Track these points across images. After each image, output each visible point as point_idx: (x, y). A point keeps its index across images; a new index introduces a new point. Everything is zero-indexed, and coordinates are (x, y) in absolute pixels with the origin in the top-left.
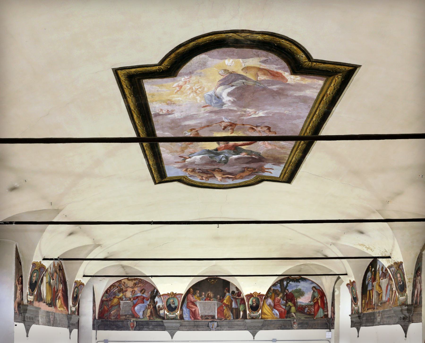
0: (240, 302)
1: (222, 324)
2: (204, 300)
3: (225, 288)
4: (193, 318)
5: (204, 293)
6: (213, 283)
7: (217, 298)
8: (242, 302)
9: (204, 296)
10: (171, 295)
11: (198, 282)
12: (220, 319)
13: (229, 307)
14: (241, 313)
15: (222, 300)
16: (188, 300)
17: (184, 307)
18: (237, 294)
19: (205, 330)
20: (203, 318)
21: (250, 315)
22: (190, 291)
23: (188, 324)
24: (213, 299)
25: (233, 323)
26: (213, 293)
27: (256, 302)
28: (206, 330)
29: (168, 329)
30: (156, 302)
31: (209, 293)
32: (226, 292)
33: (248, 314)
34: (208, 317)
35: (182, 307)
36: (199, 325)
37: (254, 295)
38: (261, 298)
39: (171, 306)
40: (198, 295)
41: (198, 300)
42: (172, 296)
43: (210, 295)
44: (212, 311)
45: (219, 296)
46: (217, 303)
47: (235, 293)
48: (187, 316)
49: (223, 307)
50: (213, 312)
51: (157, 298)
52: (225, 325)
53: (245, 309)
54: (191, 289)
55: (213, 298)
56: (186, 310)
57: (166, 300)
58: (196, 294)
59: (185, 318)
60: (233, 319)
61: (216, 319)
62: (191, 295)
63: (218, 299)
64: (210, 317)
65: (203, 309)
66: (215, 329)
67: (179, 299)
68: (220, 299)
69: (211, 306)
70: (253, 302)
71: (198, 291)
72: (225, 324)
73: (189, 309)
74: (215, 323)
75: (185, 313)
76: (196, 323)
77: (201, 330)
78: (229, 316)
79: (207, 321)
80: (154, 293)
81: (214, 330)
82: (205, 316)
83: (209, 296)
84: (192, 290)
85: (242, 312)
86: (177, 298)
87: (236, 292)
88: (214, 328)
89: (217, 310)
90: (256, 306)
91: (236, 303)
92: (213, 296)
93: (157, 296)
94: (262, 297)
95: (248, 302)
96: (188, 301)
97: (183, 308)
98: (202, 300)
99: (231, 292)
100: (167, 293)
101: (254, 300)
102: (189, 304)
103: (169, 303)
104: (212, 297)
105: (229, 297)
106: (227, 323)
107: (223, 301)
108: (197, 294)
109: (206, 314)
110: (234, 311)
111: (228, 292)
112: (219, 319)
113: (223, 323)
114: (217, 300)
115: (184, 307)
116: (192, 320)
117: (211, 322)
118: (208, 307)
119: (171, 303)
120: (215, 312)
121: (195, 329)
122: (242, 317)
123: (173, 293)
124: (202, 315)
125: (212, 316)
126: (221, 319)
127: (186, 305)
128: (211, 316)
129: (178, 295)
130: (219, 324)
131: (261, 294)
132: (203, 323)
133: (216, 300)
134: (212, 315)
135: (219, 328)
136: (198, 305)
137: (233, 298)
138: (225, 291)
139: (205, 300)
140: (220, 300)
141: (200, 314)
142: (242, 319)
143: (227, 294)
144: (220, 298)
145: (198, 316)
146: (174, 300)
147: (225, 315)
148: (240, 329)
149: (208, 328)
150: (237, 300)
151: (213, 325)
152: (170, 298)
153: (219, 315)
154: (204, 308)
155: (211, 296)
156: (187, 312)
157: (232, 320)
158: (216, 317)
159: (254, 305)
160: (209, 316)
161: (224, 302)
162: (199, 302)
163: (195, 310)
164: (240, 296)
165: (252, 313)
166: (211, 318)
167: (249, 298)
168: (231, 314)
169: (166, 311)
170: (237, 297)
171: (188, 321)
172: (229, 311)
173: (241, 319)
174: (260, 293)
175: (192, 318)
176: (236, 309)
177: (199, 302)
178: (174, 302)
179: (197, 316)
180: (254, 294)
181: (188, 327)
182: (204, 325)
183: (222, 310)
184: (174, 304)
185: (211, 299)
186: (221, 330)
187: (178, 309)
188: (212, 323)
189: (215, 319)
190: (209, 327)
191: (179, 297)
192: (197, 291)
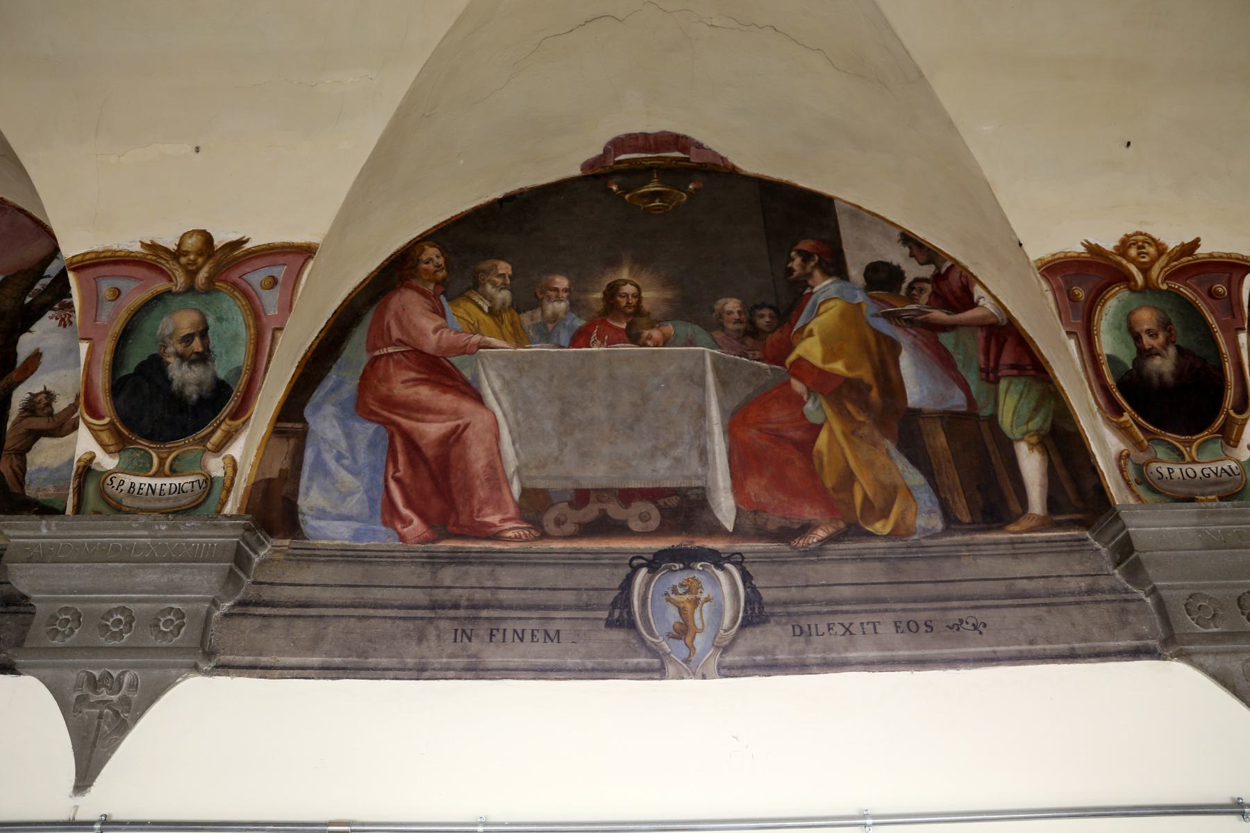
0: (987, 352)
1: (810, 593)
2: (565, 337)
3: (796, 244)
4: (416, 521)
5: (562, 282)
6: (657, 208)
7: (713, 324)
8: (998, 357)
9: (561, 306)
10: (184, 267)
11: (509, 199)
12: (775, 522)
13: (865, 406)
14: (1031, 465)
15: (777, 335)
16: (379, 336)
17: (329, 409)
18: (928, 287)
19: (570, 662)
20: (549, 518)
21: (1140, 468)
22: (419, 261)
23: (347, 595)
24: (669, 328)
25: (949, 569)
26: (667, 283)
27: (1168, 341)
28: (589, 664)
29: (56, 642)
30: (21, 359)
31: (626, 282)
32: (810, 275)
33: (1121, 458)
34: (615, 510)
35: (303, 405)
36: (487, 606)
37: (1133, 269)
38: (1212, 294)
39: (170, 382)
40: (504, 296)
41: (494, 341)
42: (192, 274)
43: (638, 296)
44: (673, 445)
45: (732, 305)
46: (716, 361)
47: (909, 277)
48: (345, 496)
49: (802, 403)
50: (678, 452)
51: (55, 322)
52: (859, 601)
53: (1053, 425)
54: (431, 252)
55: (666, 319)
56: (349, 436)
57: (113, 318)
58: (476, 286)
59: (322, 514)
60: (937, 523)
61: (729, 526)
62: (423, 293)
63: (721, 327)
64: (640, 507)
65: (548, 425)
66: (726, 650)
67: (270, 301)
68: (751, 331)
69: (645, 399)
70: (1137, 338)
71: (504, 268)
72: (847, 592)
73: (387, 423)
74: (715, 582)
75: (332, 464)
76: (448, 575)
77: (516, 661)
78: (891, 493)
79: (597, 554)
80: (38, 287)
81: (713, 659)
82: (582, 497)
83: (623, 302)
84: (441, 261)
85: (1031, 446)
86: (246, 295)
87: (913, 270)
88: (700, 641)
89: (731, 431)
90: (1179, 372)
91: (944, 360)
92: (668, 301)
93: (50, 313)
94: (1221, 288)
95: (1088, 337)
96: (377, 353)
97: (307, 412)
98: (545, 335)
99: (856, 273)
100: (137, 248)
101: (1146, 318)
102: (387, 379)
103: (154, 350)
104: (656, 314)
105: (843, 315)
106: (877, 571)
107: (791, 348)
108: (489, 288)
109: (596, 474)
110: (939, 441)
111: (827, 274)
112: (762, 534)
113: (820, 572)
114: (718, 335)
115: (329, 409)
116: (402, 538)
117: (655, 562)
118: (612, 406)
119: (170, 350)
120: (704, 455)
121: (431, 651)
122: (1053, 503)
123: (207, 238)
124: (541, 485)
125: (673, 501)
126: (785, 535)
127: (350, 387)
128: (652, 495)
129: (258, 263)
130: (767, 595)
131: (1202, 251)
132: (548, 575)
133: (702, 335)
134: (668, 484)
135: (773, 637)
136: (497, 384)
137: (889, 316)
138: (796, 263)
139: (581, 338)
140: (749, 341)
141: (518, 471)
142: (1058, 525)
143: (823, 285)
144: (752, 323)
145: (484, 503)
146: (211, 320)
147: (829, 481)
148: (1062, 647)
149: (618, 635)
150: (946, 339)
151: (696, 602)
152: (169, 292)
153: (754, 487)
154: (564, 414)
155: (646, 306)
156: (352, 449)
157: (934, 536)
158: (725, 508)
159: (1163, 365)
160: (627, 496)
161: (799, 351)
162: (501, 356)
163: (455, 437)
164: (972, 304)
165: (1161, 452)
166: (654, 523)
167: (1080, 293)
168: (914, 478)
169: (86, 423)
170: (938, 315)
171: (348, 556)
172: (875, 444)
173: (1045, 525)
174: (1196, 243)
175: (411, 522)
176: (951, 420)
177: (508, 358)
178: (204, 334)
179: (469, 491)
180: (1133, 252)
181: (333, 629)
182: (567, 597)
183: (797, 435)
184: (204, 358)
185: (646, 333)
186: (802, 667)
187: (242, 411)
188: (677, 579)
189: (716, 530)
190: (632, 625)
191: (274, 282)
192: (486, 265)
